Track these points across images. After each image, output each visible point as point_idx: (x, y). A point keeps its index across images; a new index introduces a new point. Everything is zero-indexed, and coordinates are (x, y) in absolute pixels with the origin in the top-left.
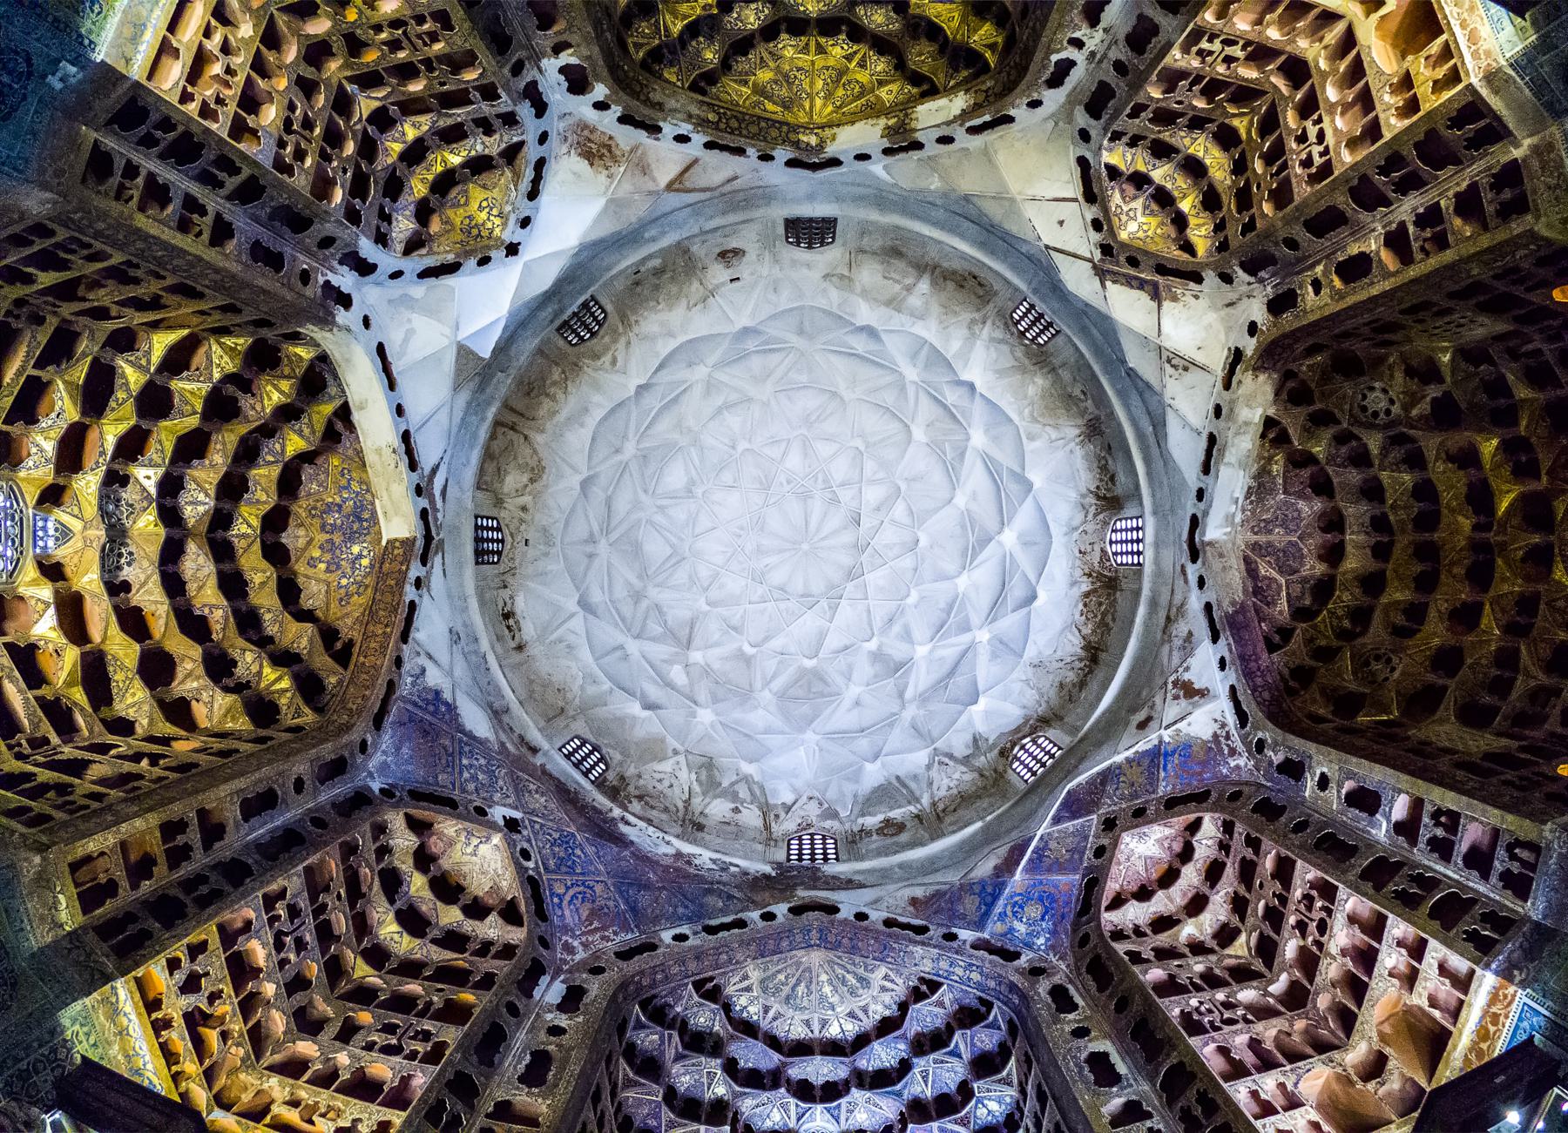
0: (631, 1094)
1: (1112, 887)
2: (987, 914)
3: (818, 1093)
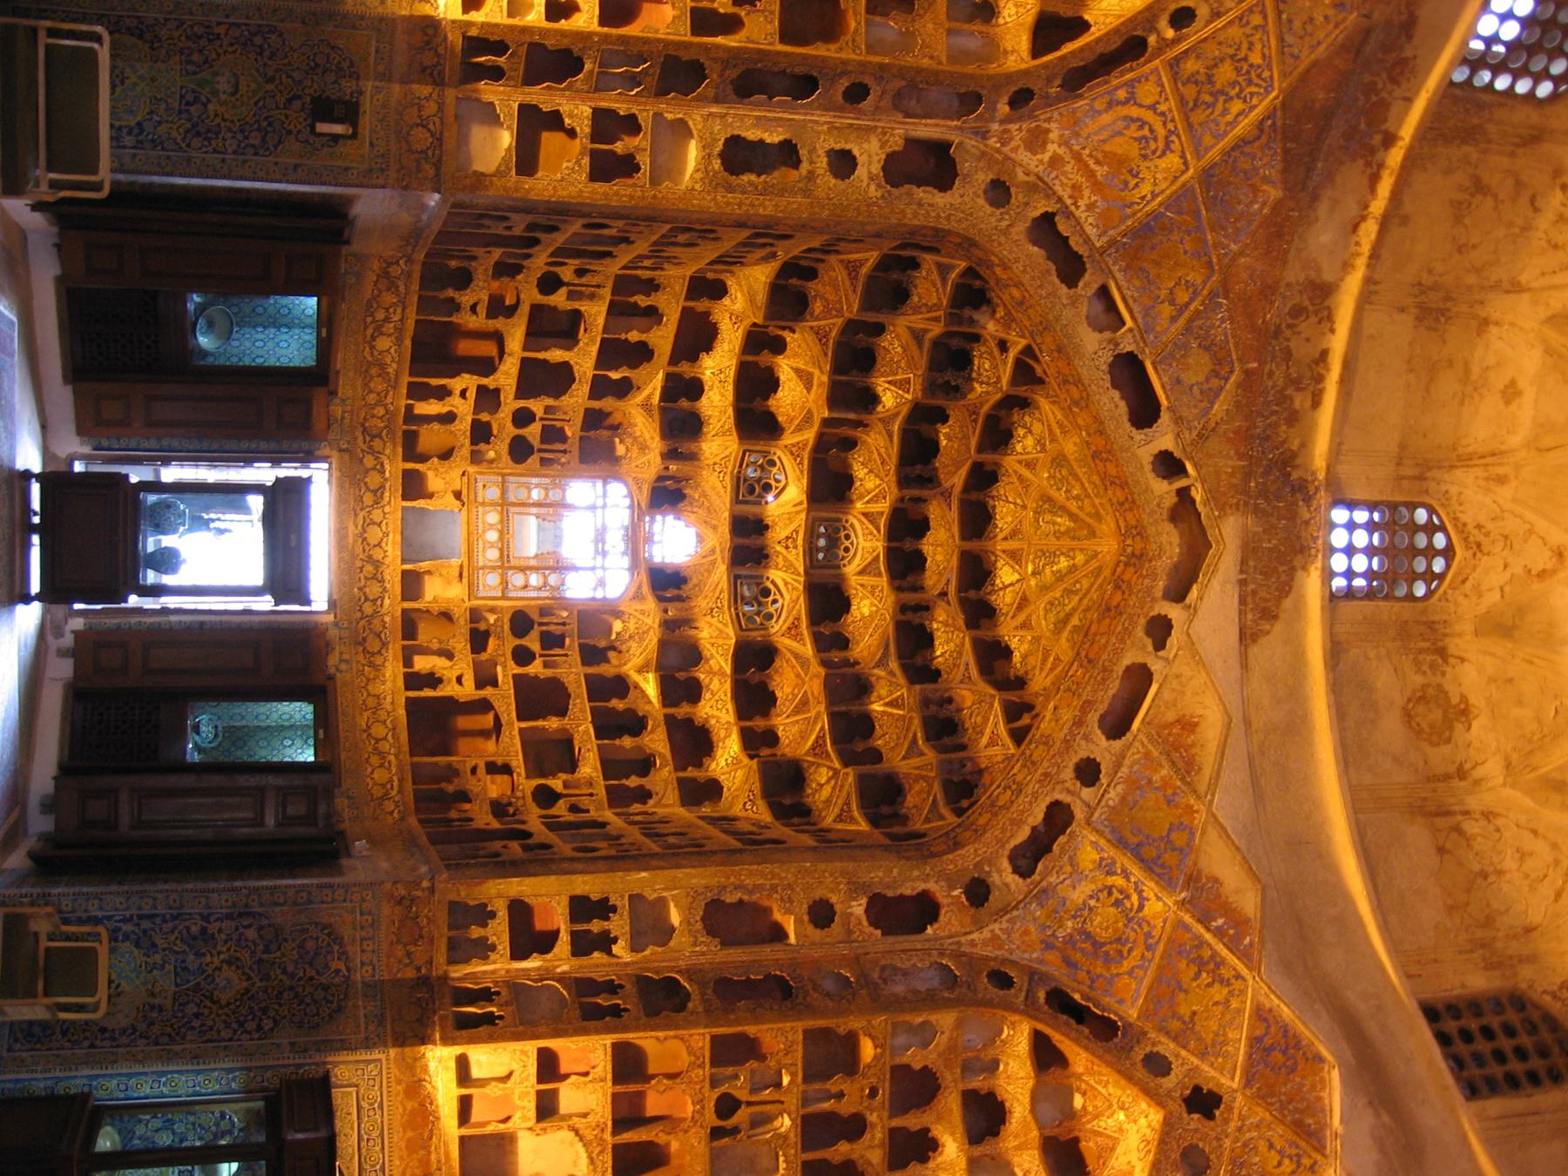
0: (840, 274)
2: (1120, 843)
3: (908, 545)
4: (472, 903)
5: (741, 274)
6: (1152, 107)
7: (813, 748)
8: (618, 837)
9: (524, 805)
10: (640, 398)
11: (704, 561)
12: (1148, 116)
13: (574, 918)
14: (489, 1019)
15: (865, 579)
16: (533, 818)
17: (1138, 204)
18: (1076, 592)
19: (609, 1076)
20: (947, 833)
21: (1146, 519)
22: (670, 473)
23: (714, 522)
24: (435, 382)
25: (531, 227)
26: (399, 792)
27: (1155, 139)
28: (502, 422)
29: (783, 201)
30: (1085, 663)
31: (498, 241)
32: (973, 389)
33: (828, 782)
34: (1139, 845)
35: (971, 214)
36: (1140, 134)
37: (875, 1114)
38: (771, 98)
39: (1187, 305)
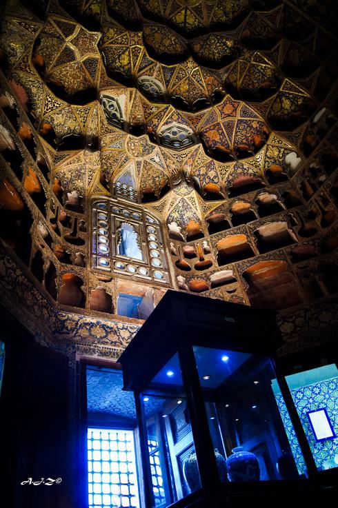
9: (318, 239)
11: (140, 176)
15: (172, 82)
23: (123, 159)
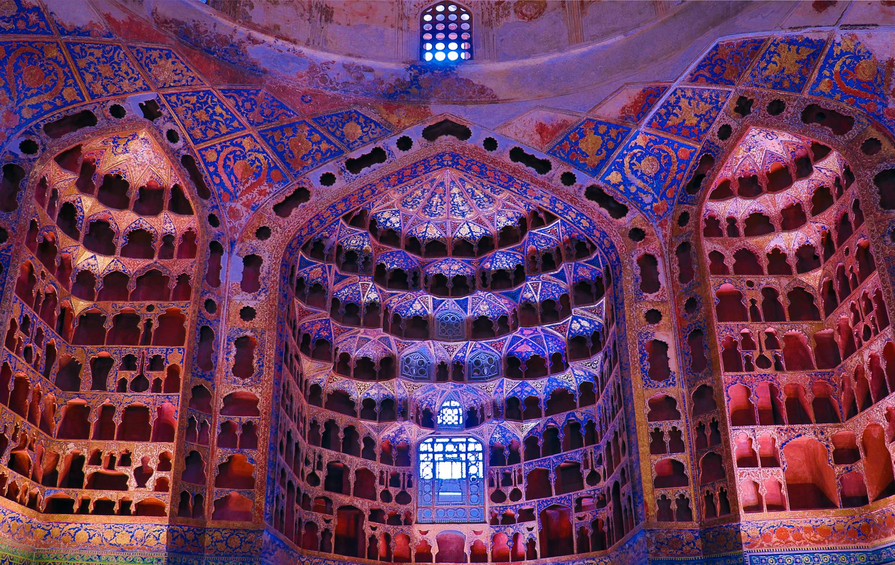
0: (306, 320)
1: (727, 172)
3: (450, 285)
4: (657, 509)
5: (307, 375)
6: (219, 153)
7: (561, 332)
8: (616, 433)
9: (598, 490)
10: (375, 434)
12: (223, 154)
13: (663, 451)
14: (723, 495)
15: (470, 306)
16: (604, 484)
17: (268, 160)
18: (473, 192)
19: (751, 427)
20: (606, 253)
21: (434, 153)
22: (415, 416)
24: (367, 545)
25: (282, 484)
26: (594, 560)
27: (235, 152)
28: (388, 507)
29: (268, 345)
30: (511, 183)
31: (290, 505)
32: (367, 251)
33: (579, 323)
34: (607, 149)
35: (274, 246)
36: (232, 160)
37: (762, 282)
38: (213, 352)
39: (321, 134)
